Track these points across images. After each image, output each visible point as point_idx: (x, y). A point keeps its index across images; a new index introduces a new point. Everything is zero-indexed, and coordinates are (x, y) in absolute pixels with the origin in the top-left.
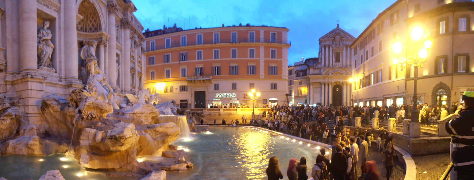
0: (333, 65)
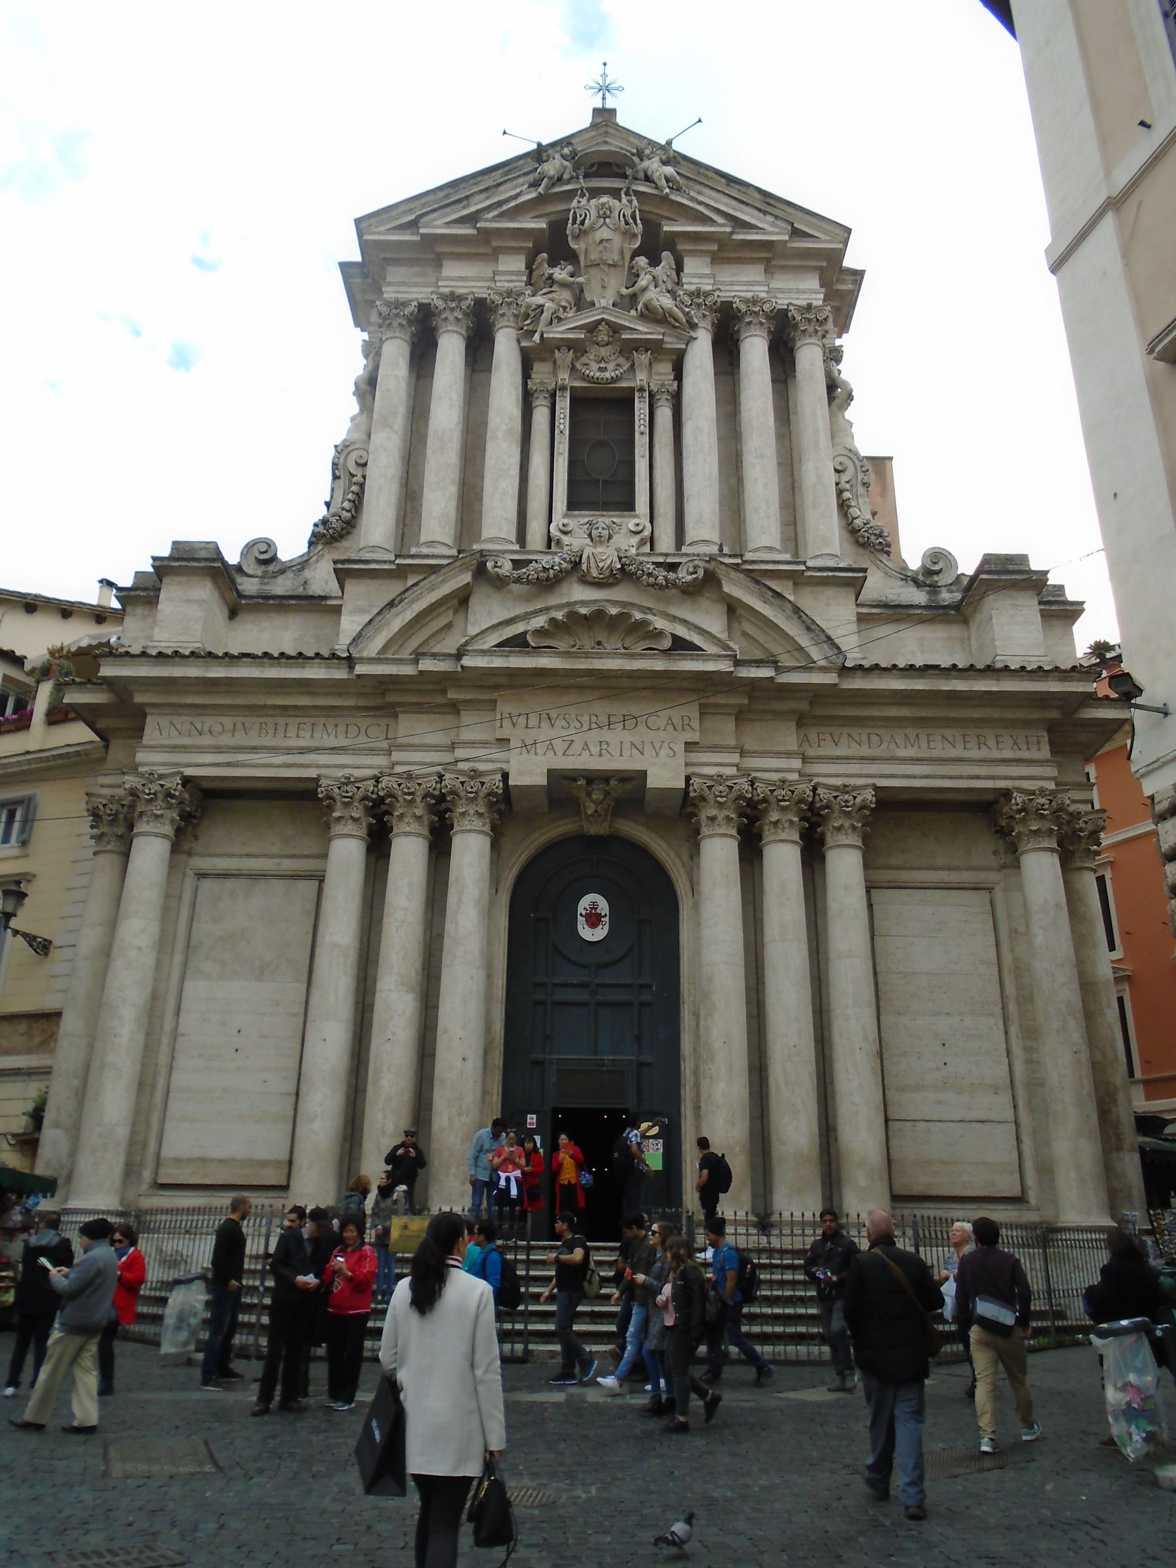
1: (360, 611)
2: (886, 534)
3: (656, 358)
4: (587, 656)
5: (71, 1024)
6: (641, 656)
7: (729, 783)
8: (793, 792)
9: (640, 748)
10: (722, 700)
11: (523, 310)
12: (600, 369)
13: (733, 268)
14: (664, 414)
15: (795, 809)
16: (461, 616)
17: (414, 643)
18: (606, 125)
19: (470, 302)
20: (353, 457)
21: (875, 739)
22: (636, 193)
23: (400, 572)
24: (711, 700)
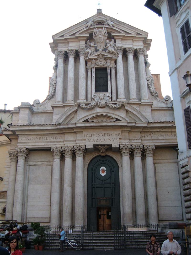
0: (89, 100)
1: (57, 114)
2: (157, 93)
3: (111, 61)
4: (100, 123)
5: (10, 194)
6: (110, 122)
7: (127, 146)
8: (139, 147)
9: (110, 140)
10: (126, 130)
11: (85, 53)
12: (100, 63)
13: (126, 41)
14: (113, 71)
15: (140, 150)
16: (76, 115)
17: (67, 121)
18: (100, 13)
19: (75, 51)
20: (54, 81)
21: (155, 135)
22: (106, 28)
23: (64, 107)
24: (124, 130)
